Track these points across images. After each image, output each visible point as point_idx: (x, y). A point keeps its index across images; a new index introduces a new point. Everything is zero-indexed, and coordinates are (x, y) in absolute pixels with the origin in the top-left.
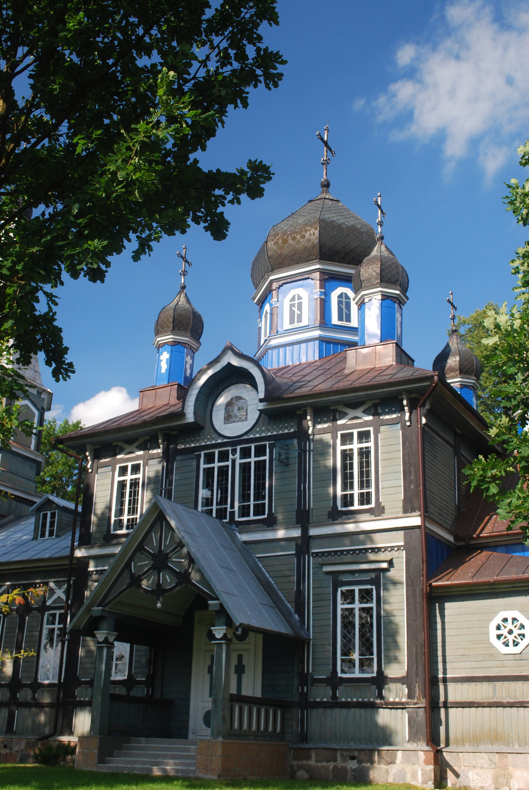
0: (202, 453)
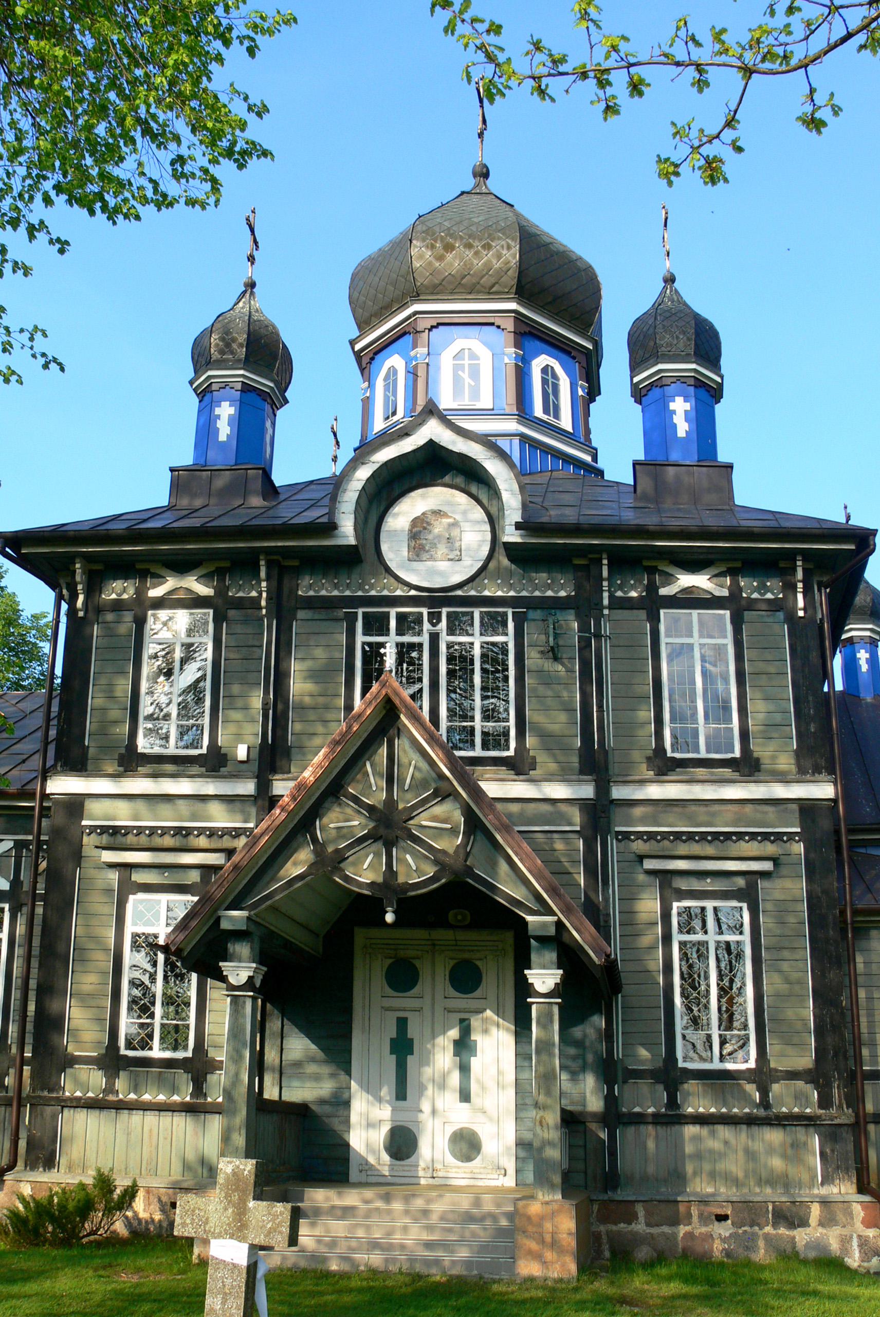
0: (360, 611)
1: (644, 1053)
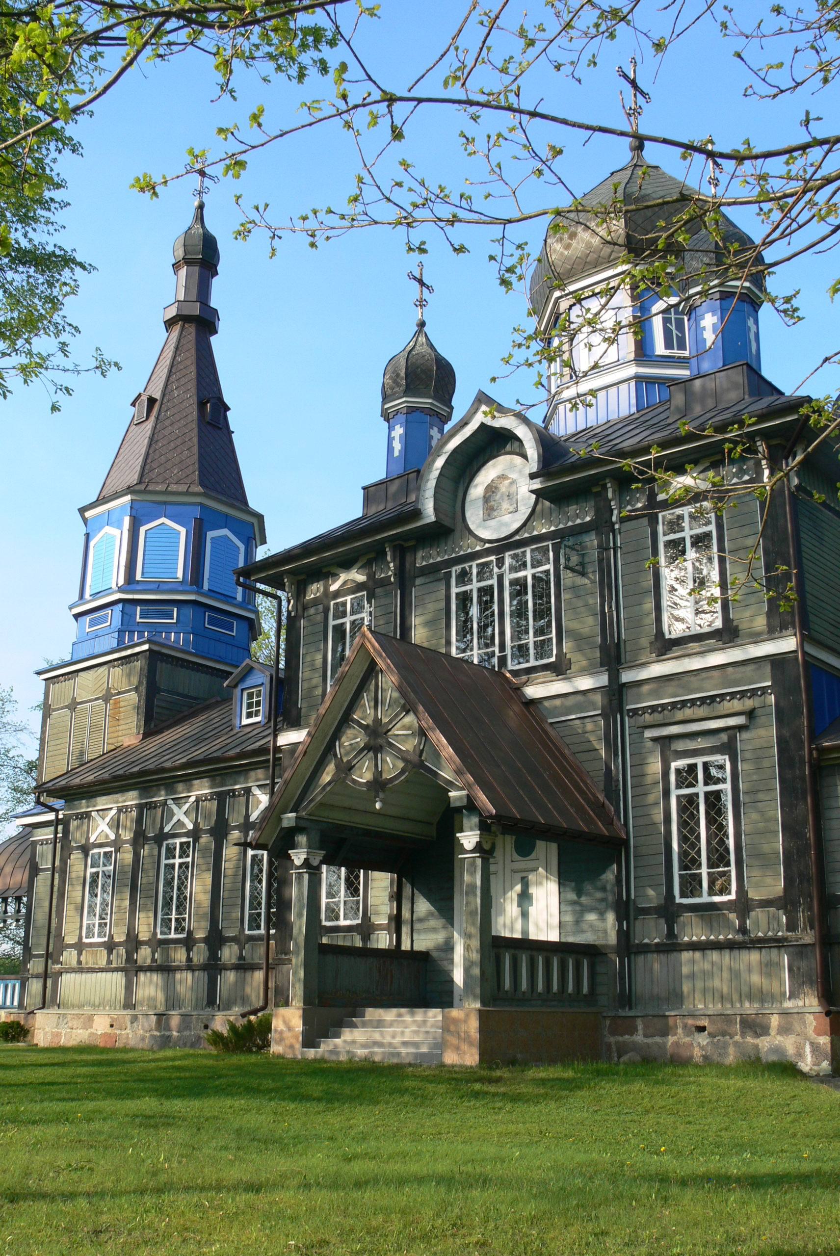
1: (651, 892)
